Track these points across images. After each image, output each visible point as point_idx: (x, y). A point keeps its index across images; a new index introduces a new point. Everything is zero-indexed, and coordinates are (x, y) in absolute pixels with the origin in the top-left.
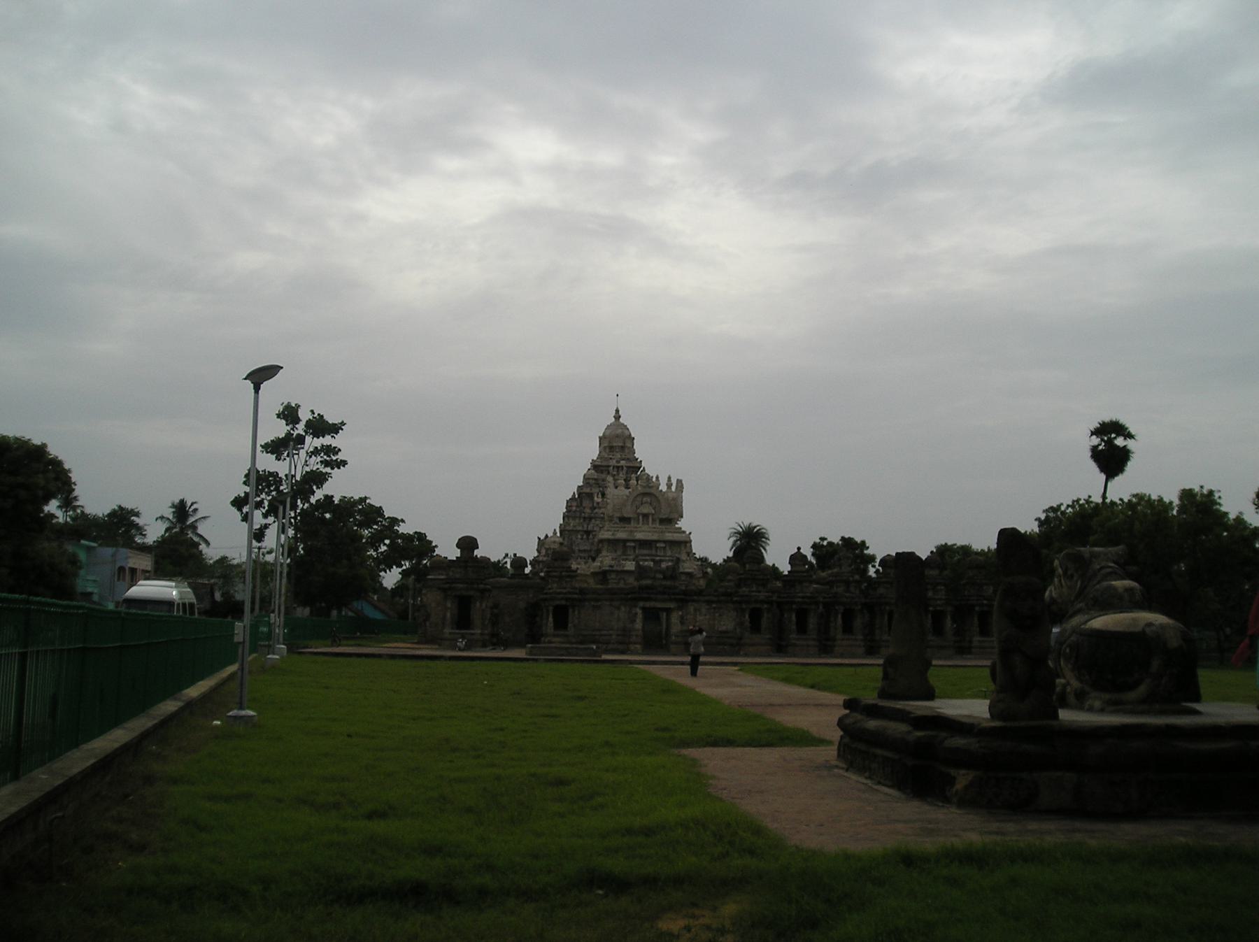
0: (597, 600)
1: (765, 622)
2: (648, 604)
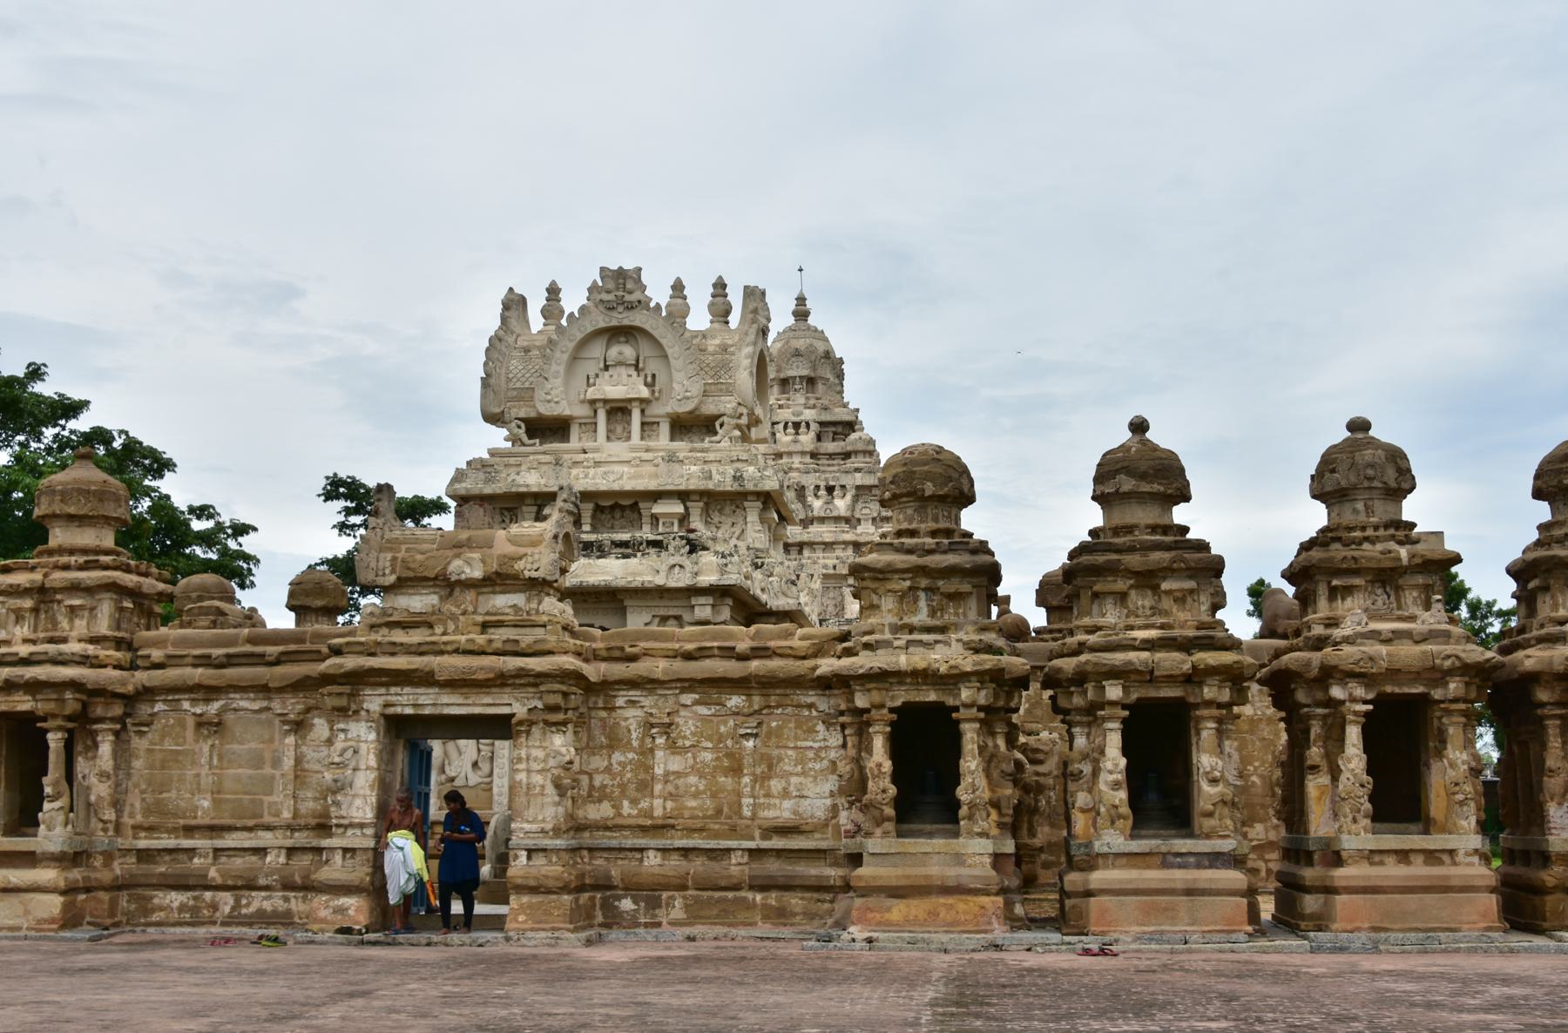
0: (209, 692)
1: (972, 779)
2: (406, 701)
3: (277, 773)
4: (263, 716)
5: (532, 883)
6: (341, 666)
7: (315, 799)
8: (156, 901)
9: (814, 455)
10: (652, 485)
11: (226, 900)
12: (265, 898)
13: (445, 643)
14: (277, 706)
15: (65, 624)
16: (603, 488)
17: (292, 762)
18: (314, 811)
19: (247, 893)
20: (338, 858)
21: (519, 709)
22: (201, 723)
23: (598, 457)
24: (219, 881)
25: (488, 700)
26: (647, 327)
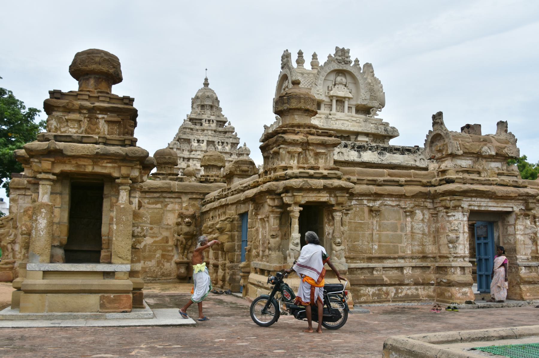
0: (378, 196)
3: (403, 234)
4: (395, 208)
5: (531, 280)
6: (461, 188)
7: (419, 245)
8: (362, 292)
9: (215, 131)
10: (360, 130)
11: (392, 290)
12: (408, 289)
13: (493, 181)
14: (402, 204)
15: (312, 161)
16: (343, 129)
17: (410, 229)
18: (418, 250)
19: (401, 287)
20: (458, 270)
21: (516, 209)
22: (371, 210)
23: (336, 117)
24: (389, 282)
25: (505, 205)
26: (352, 71)
